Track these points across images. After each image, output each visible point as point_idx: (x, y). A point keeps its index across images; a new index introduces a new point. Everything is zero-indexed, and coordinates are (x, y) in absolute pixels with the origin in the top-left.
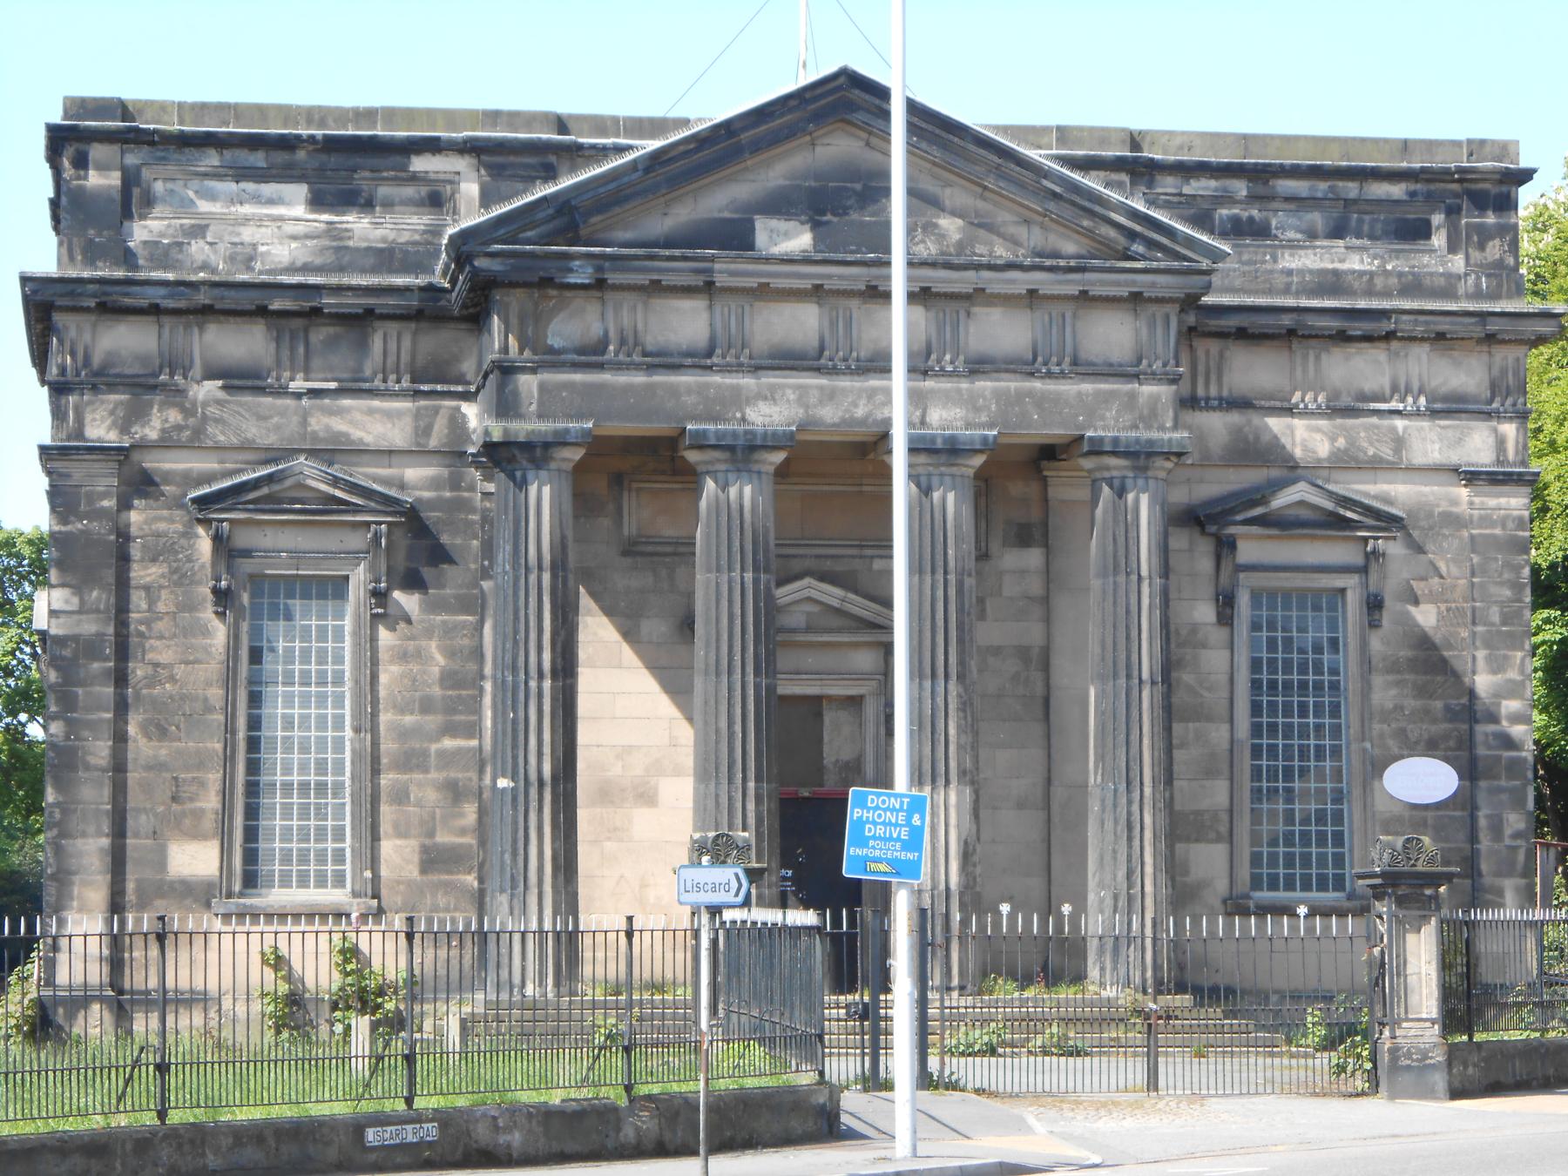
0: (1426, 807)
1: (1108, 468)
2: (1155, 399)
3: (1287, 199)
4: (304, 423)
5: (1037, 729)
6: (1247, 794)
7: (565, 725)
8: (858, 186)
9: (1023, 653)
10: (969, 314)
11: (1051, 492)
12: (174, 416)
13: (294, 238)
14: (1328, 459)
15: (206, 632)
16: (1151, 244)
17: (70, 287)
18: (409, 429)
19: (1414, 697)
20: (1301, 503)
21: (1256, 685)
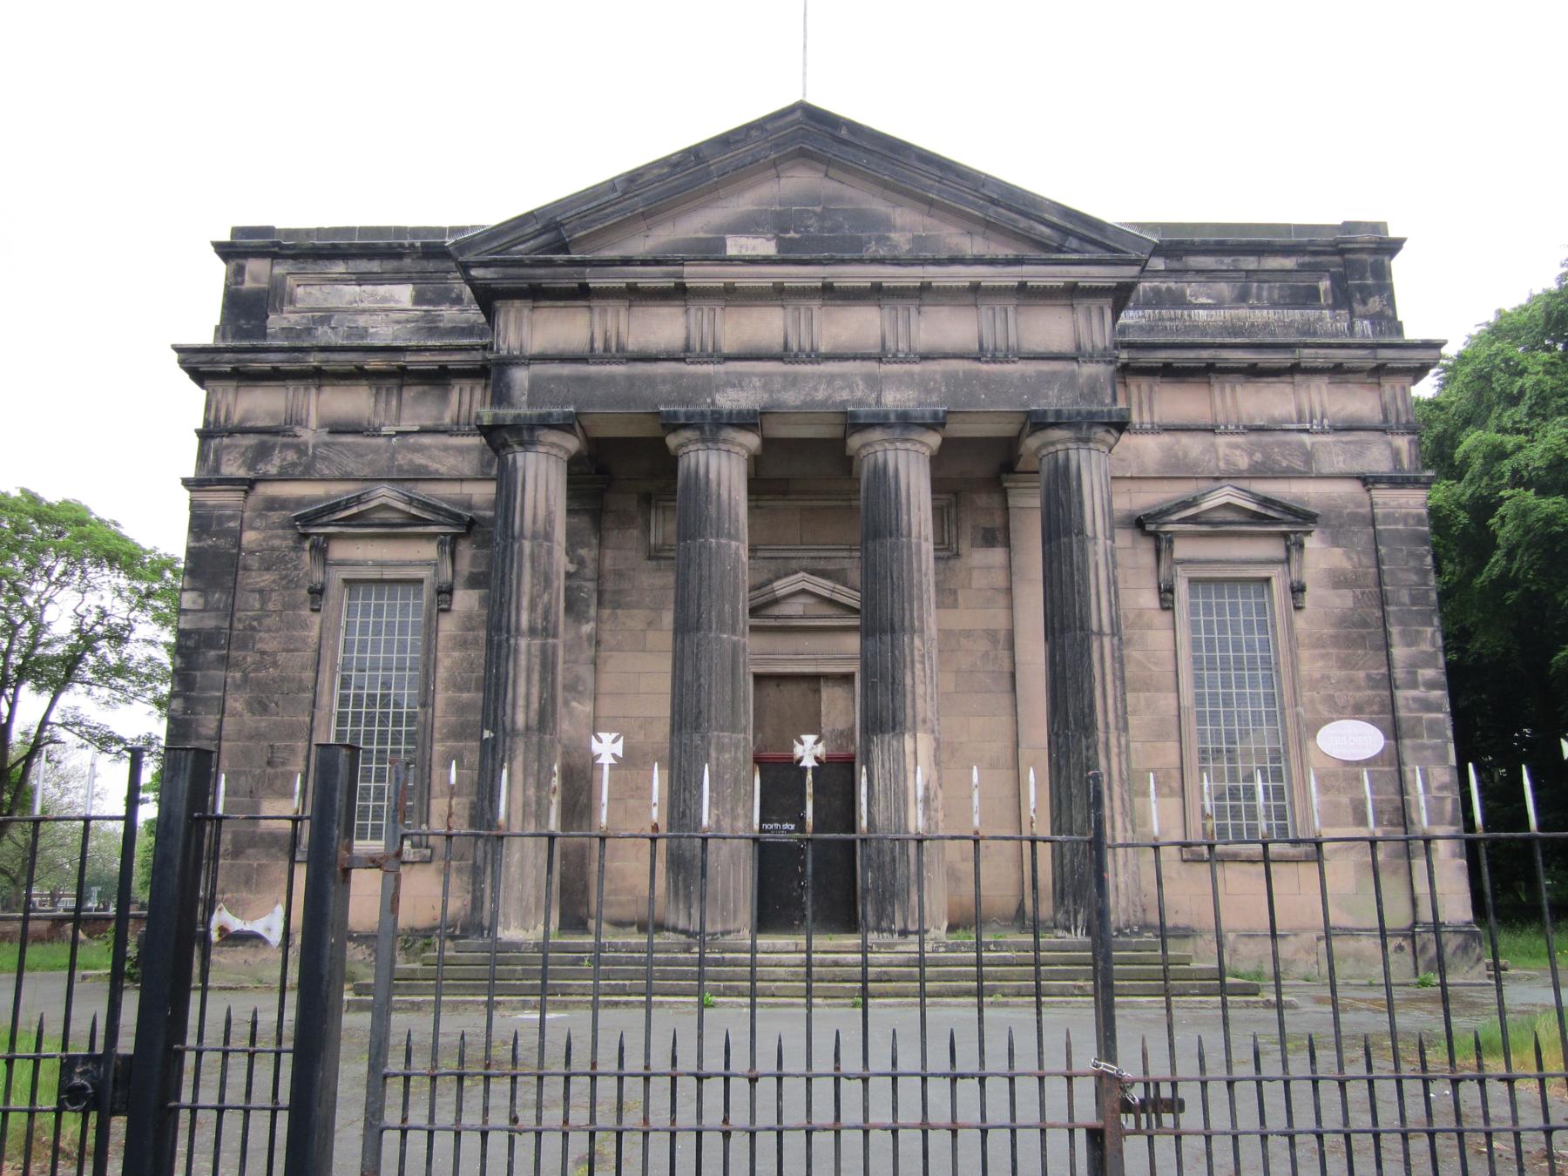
0: (1358, 763)
1: (1053, 443)
2: (1094, 379)
3: (1198, 271)
4: (393, 458)
5: (1005, 700)
7: (543, 680)
8: (818, 209)
9: (991, 635)
11: (1011, 502)
12: (291, 456)
13: (398, 322)
14: (1248, 470)
15: (305, 626)
16: (1083, 239)
17: (212, 356)
18: (476, 462)
19: (1339, 668)
21: (1197, 661)
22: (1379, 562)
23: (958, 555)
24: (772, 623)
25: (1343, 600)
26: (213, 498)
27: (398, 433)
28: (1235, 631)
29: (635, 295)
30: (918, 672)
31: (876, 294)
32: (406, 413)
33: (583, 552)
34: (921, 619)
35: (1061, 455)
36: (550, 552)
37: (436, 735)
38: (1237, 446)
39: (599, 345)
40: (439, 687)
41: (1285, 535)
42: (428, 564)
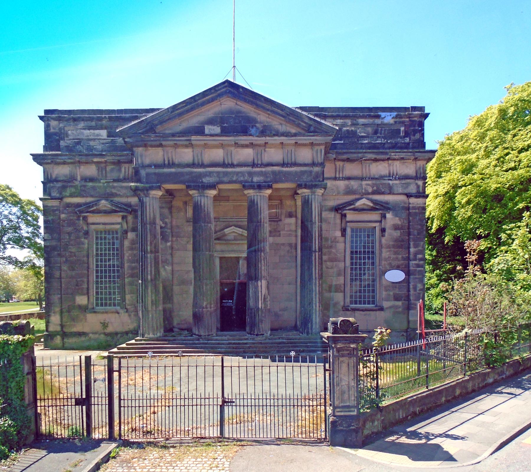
2: (317, 173)
6: (349, 280)
9: (290, 245)
15: (83, 244)
20: (364, 204)
22: (409, 222)
23: (280, 220)
25: (397, 234)
26: (51, 203)
30: (263, 263)
33: (166, 220)
35: (307, 197)
36: (155, 228)
40: (125, 262)
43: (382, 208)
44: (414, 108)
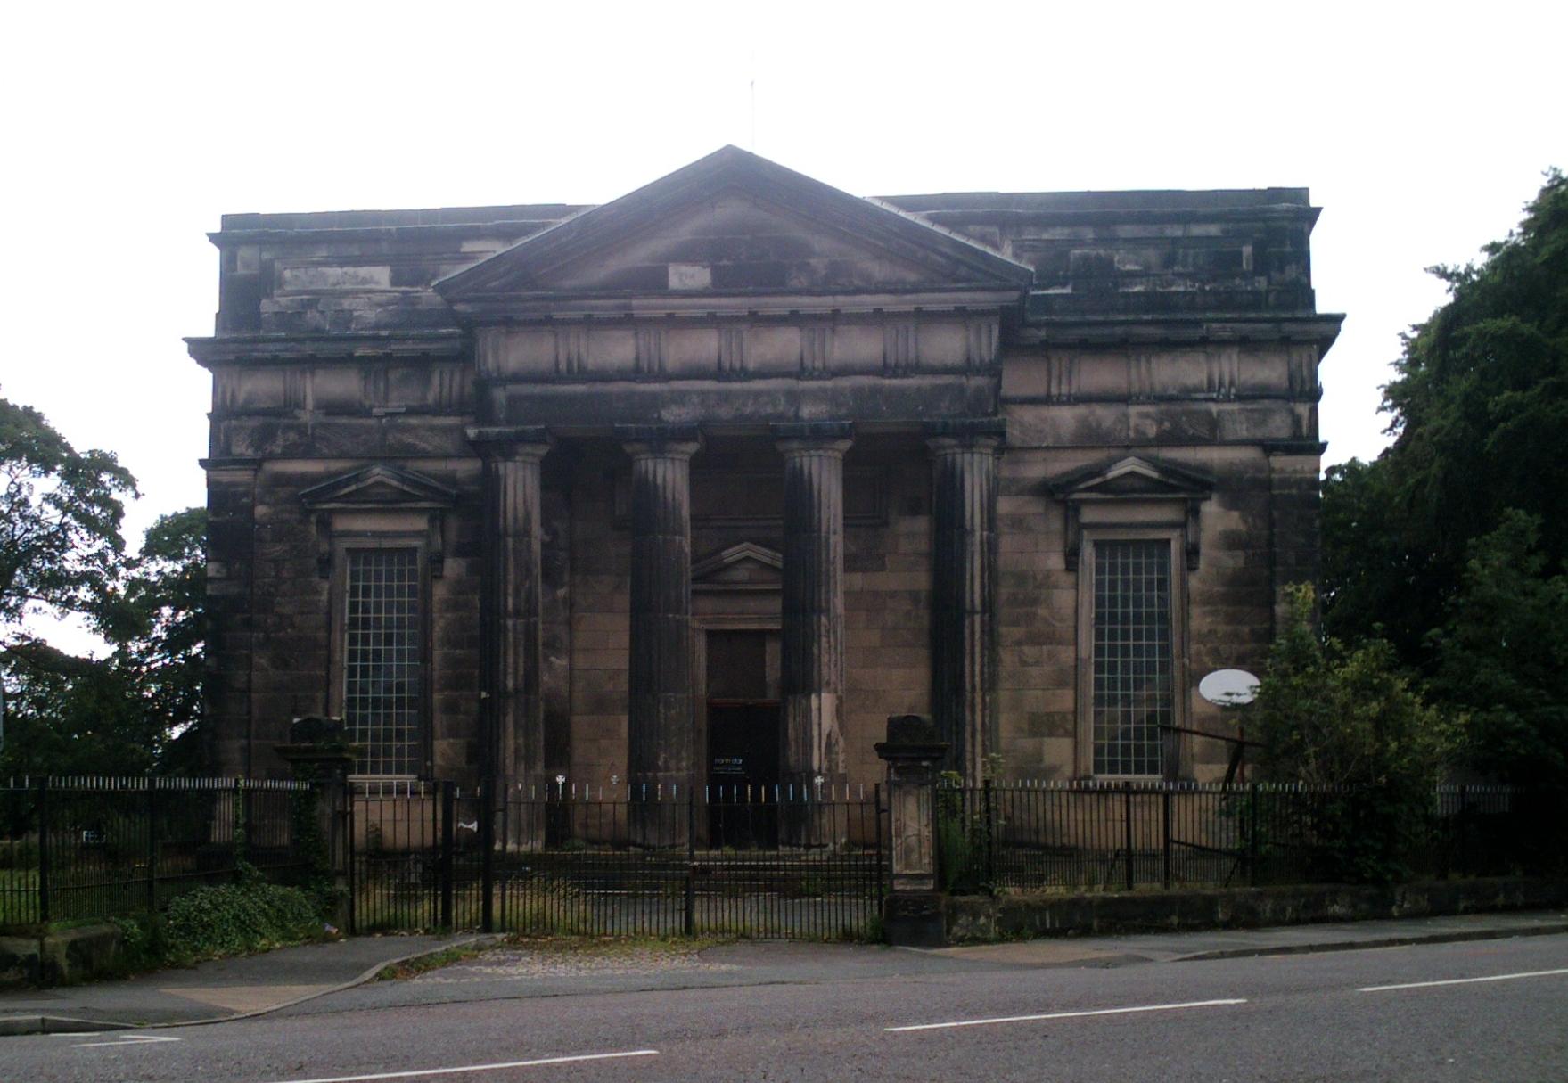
2: (979, 390)
3: (1127, 240)
10: (834, 331)
15: (317, 592)
20: (1132, 474)
22: (1272, 525)
24: (721, 588)
25: (1232, 561)
27: (387, 414)
28: (1137, 589)
29: (591, 324)
31: (794, 319)
32: (394, 395)
34: (828, 601)
35: (949, 458)
36: (529, 545)
37: (436, 686)
38: (1147, 416)
39: (563, 366)
41: (1184, 500)
42: (418, 534)
43: (1188, 487)
44: (1275, 194)
